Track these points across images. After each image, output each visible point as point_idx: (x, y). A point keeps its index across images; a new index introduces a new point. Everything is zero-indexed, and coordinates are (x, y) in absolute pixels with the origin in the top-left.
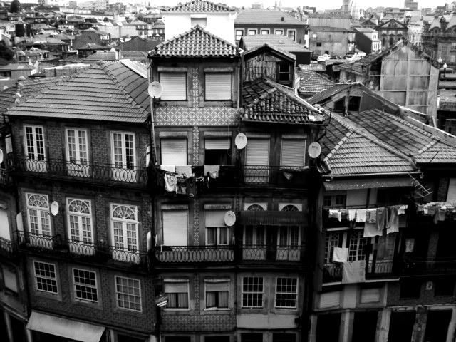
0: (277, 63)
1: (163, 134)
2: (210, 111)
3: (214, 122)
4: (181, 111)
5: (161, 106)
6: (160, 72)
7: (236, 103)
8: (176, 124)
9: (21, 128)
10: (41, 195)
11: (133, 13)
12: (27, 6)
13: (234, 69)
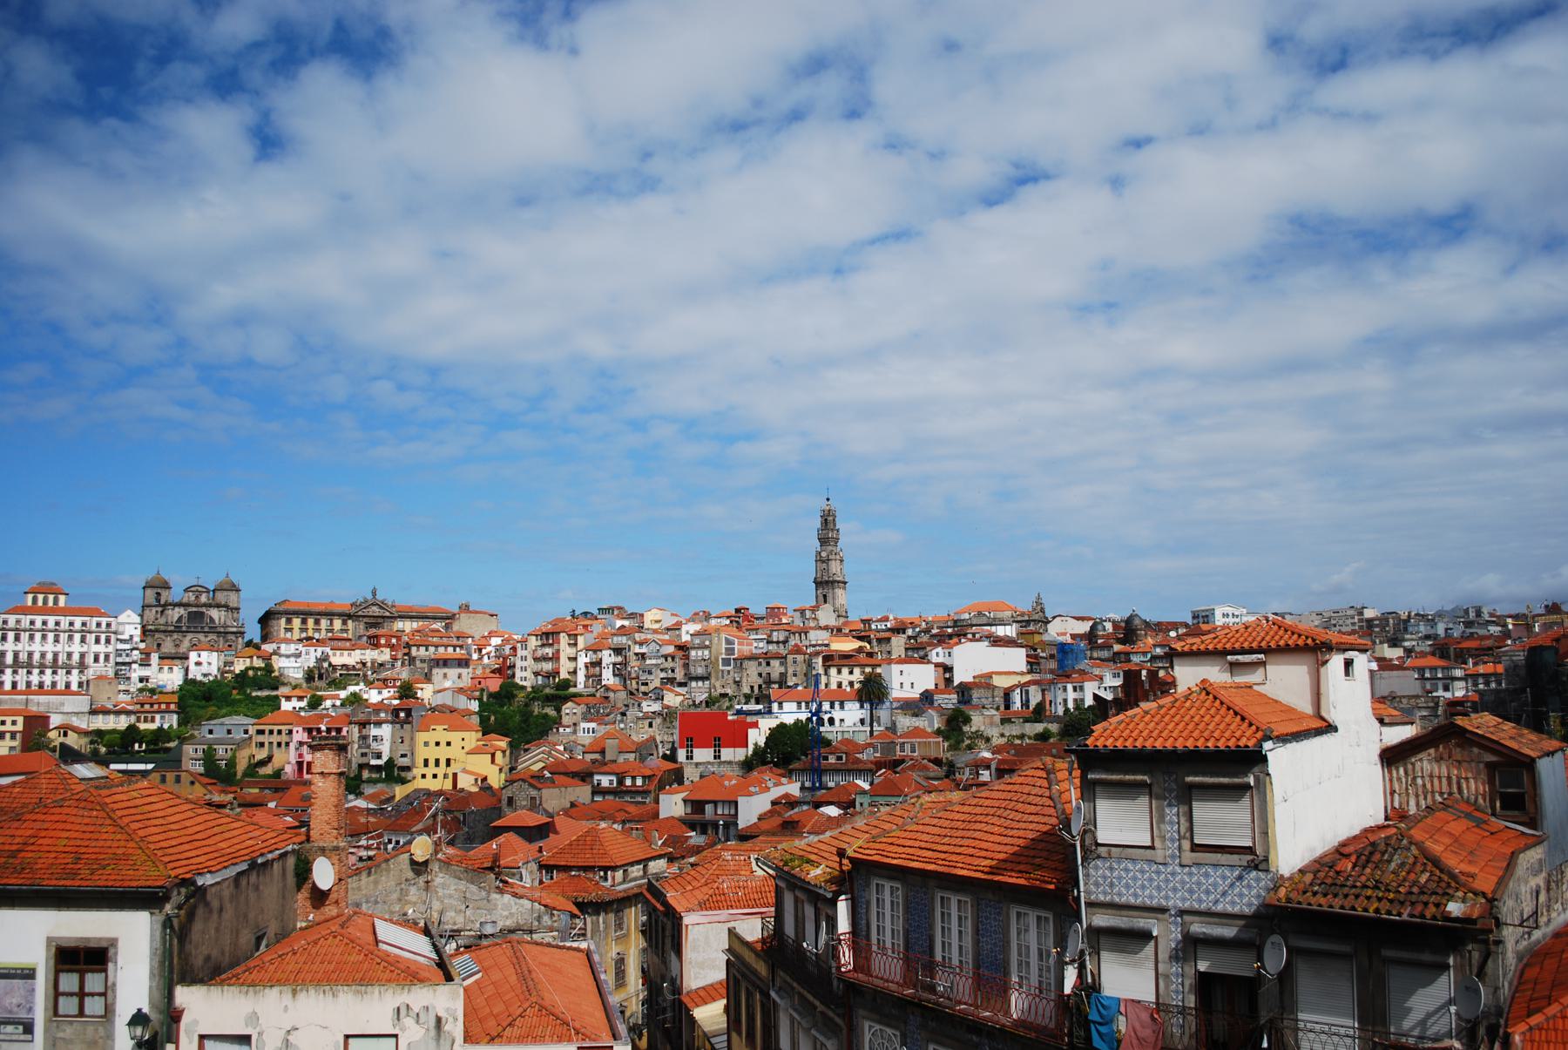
0: (1489, 765)
1: (1102, 920)
2: (1207, 875)
3: (1216, 902)
4: (1142, 872)
5: (1099, 857)
6: (1096, 783)
7: (1266, 860)
8: (1132, 900)
9: (868, 885)
10: (889, 1031)
11: (1427, 637)
12: (1161, 628)
13: (1257, 779)
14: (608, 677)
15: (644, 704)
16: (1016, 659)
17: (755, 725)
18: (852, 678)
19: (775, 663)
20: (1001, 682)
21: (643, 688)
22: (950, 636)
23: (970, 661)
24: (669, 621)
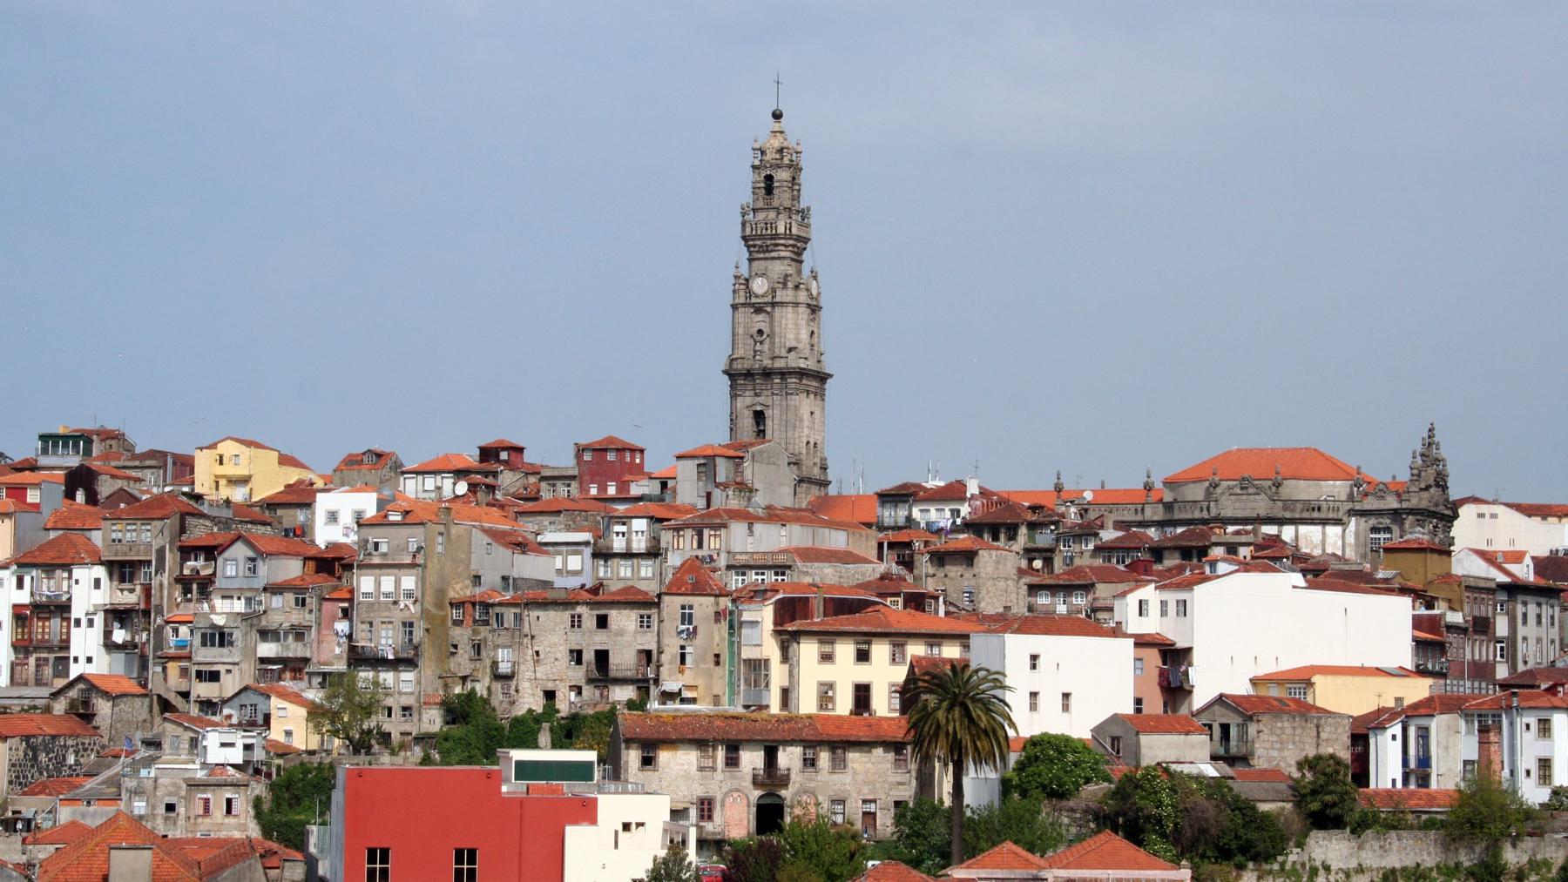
14: (88, 650)
15: (212, 740)
16: (1380, 628)
17: (586, 812)
18: (863, 673)
19: (624, 620)
20: (1344, 699)
21: (204, 690)
22: (1158, 553)
23: (1244, 627)
24: (270, 481)
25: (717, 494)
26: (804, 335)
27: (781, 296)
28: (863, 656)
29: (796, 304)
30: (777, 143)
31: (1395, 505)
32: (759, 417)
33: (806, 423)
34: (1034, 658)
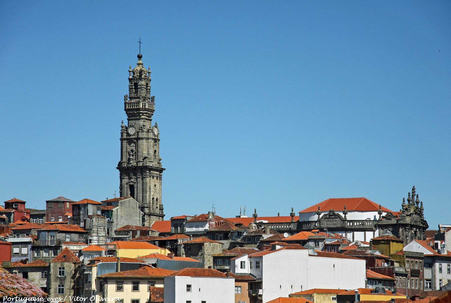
18: (136, 296)
25: (88, 220)
26: (152, 152)
27: (141, 135)
28: (136, 289)
29: (148, 139)
30: (139, 68)
31: (395, 222)
32: (132, 188)
33: (152, 190)
34: (189, 286)
